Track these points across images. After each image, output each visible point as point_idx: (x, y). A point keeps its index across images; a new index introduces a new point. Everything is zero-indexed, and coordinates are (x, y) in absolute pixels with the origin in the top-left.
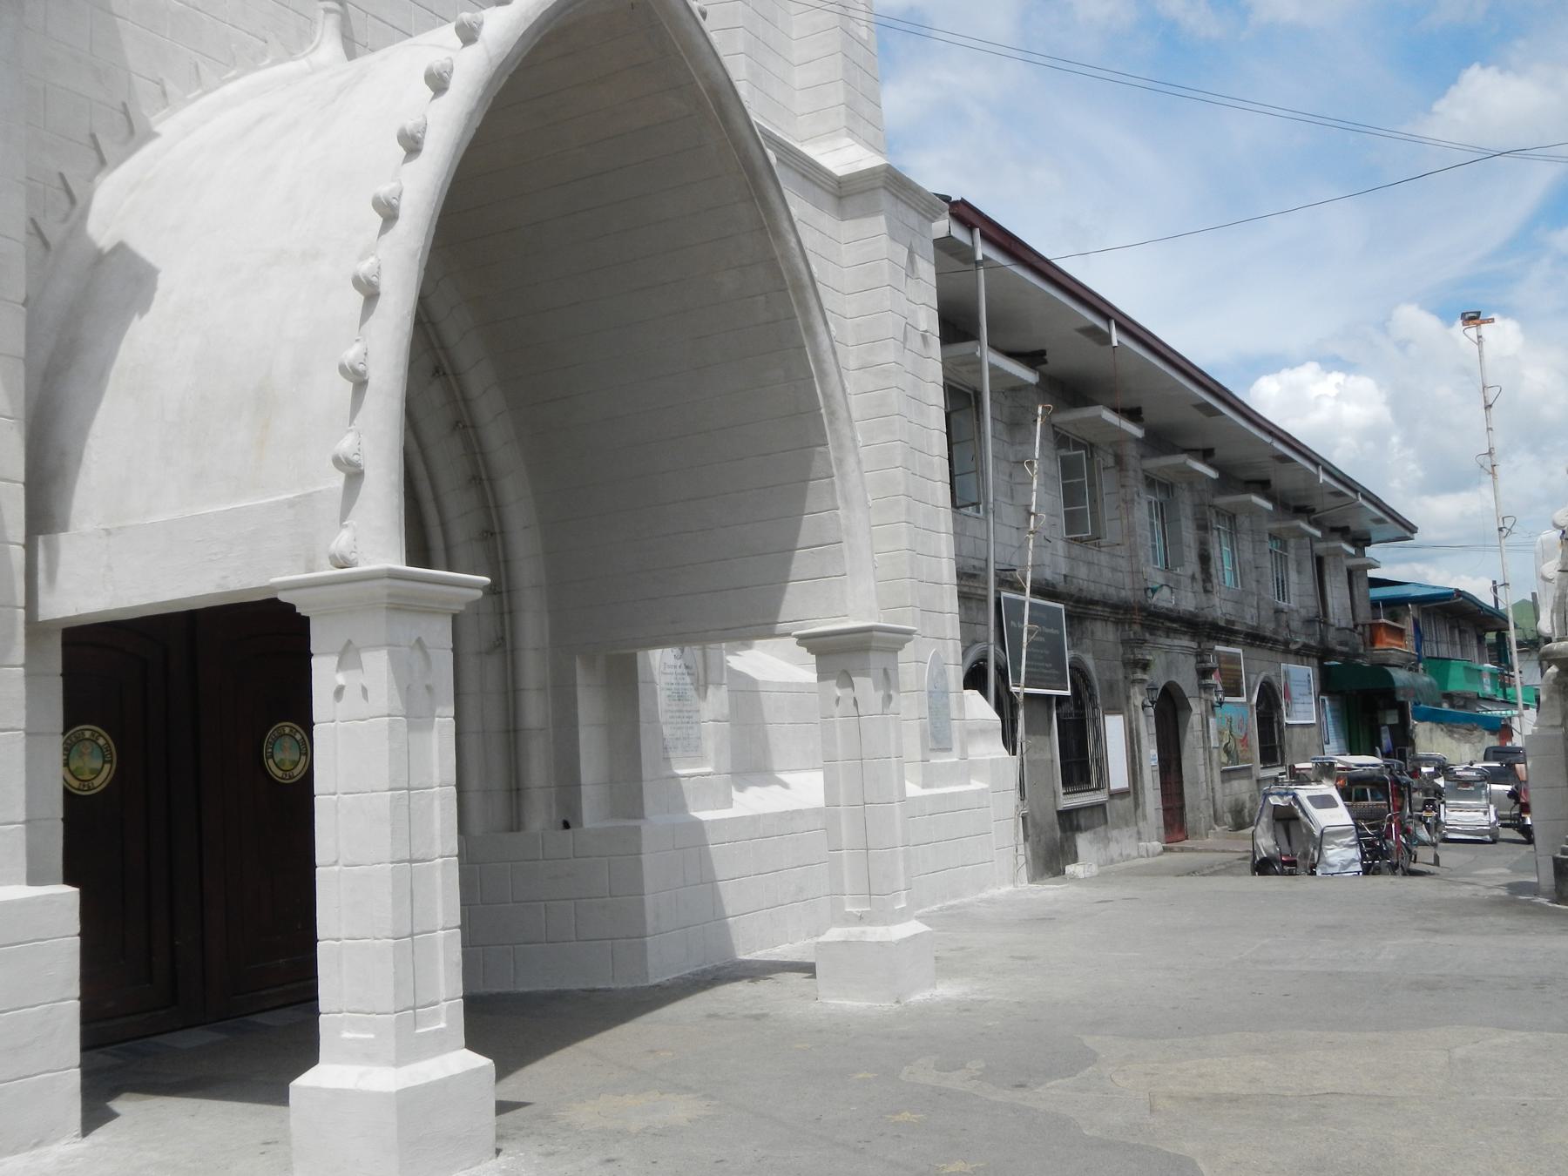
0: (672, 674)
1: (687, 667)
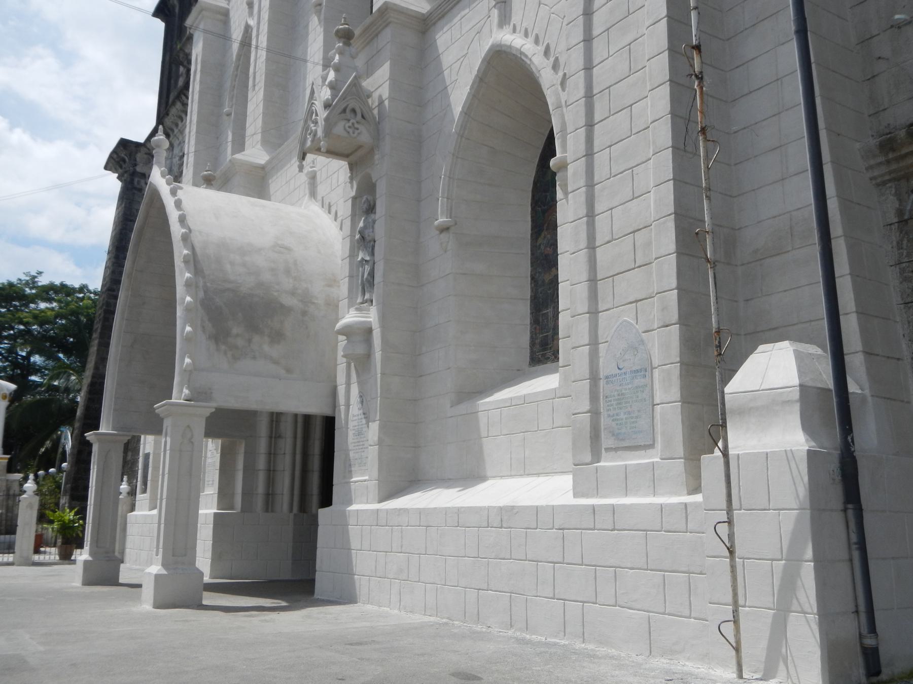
0: (355, 420)
1: (364, 414)
